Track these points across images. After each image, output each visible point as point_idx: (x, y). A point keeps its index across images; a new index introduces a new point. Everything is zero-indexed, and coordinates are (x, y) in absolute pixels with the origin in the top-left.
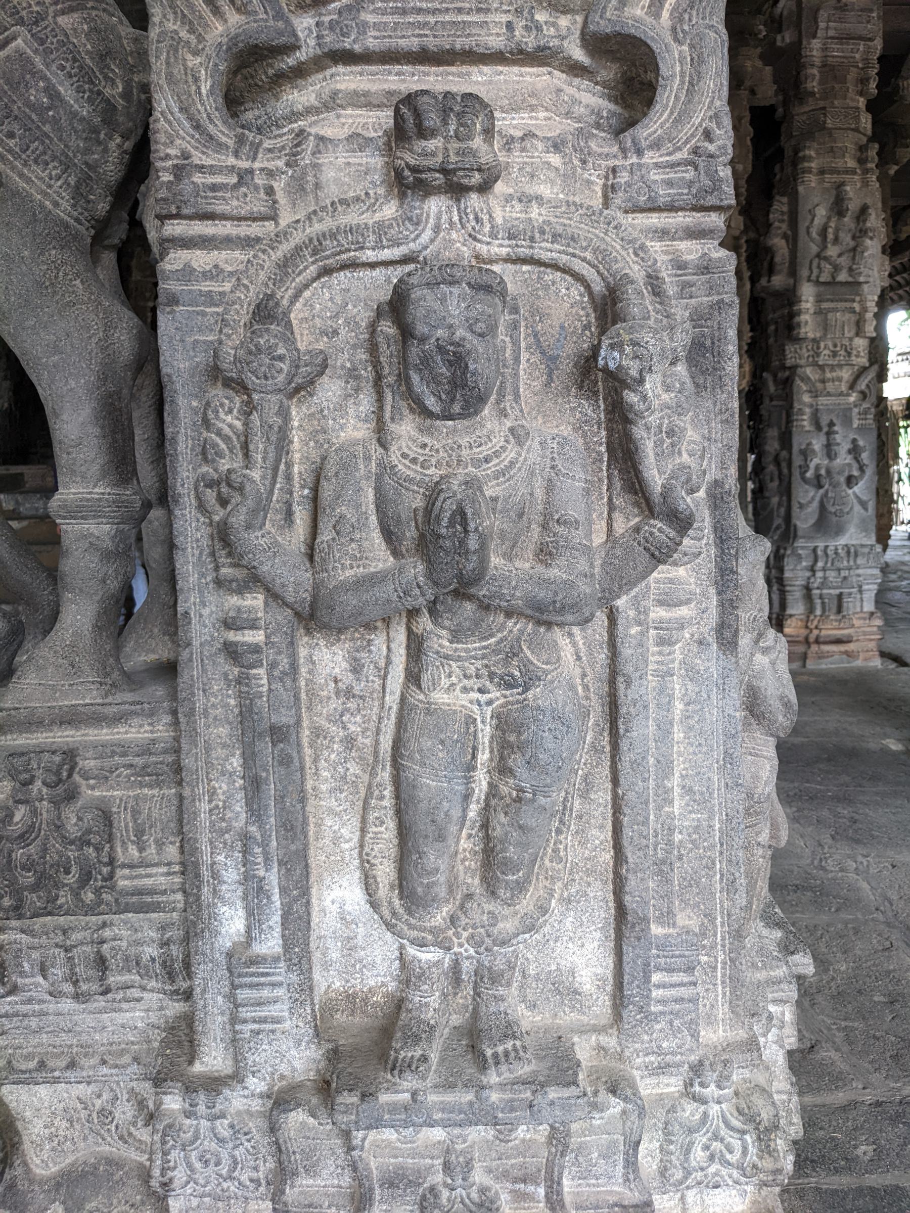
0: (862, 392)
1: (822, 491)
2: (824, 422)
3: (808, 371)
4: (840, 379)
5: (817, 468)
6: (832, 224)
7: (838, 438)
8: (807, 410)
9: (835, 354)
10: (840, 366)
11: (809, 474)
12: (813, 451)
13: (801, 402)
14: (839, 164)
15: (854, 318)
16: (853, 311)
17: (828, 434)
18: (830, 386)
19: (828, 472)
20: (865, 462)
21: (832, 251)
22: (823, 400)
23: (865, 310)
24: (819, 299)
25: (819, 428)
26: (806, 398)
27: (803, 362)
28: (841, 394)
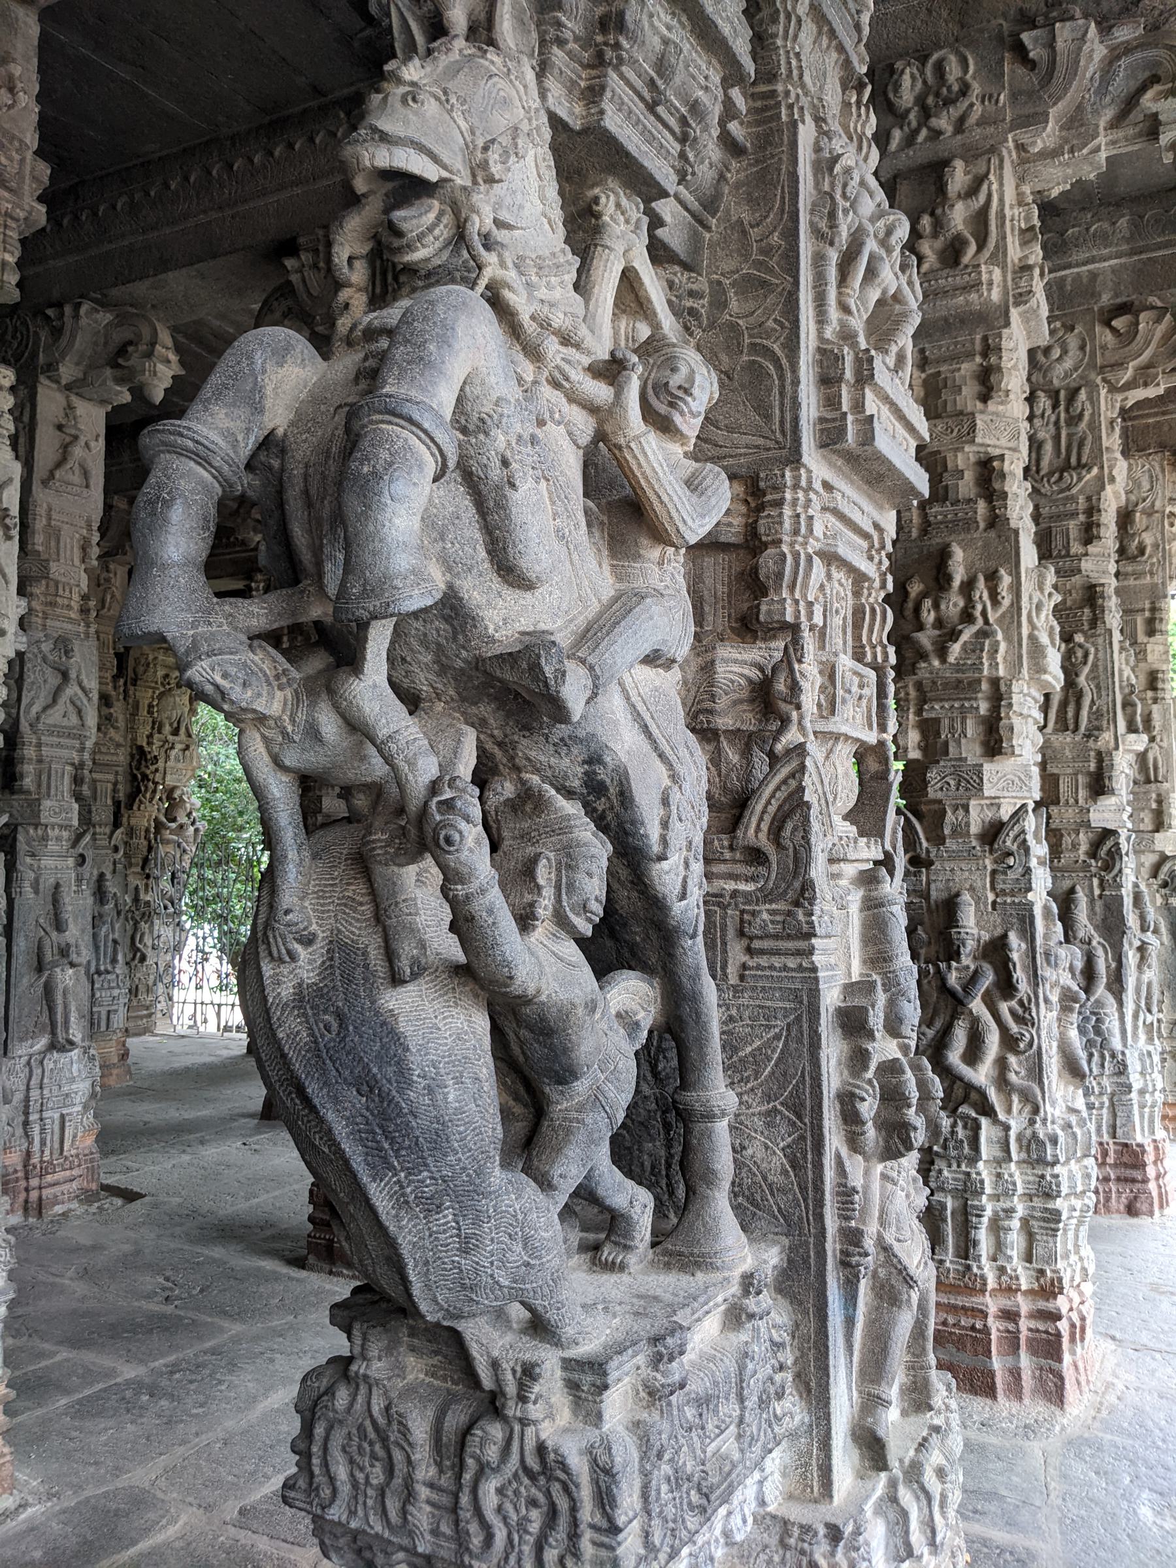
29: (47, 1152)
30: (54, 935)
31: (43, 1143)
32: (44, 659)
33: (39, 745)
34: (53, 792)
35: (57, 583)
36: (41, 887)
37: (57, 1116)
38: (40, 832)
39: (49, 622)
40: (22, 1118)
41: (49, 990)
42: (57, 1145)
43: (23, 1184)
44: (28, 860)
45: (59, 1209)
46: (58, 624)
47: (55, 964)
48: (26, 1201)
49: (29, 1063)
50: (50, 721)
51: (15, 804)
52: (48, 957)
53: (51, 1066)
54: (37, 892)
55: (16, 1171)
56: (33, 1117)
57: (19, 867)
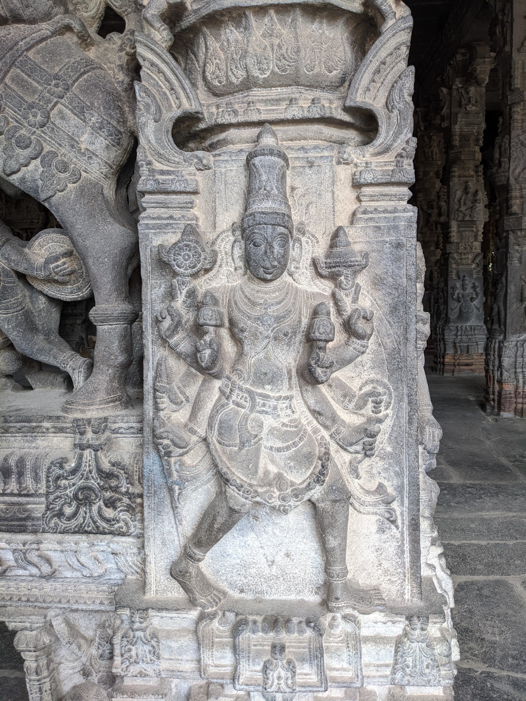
1: (460, 304)
2: (461, 275)
3: (455, 255)
4: (468, 258)
5: (458, 294)
6: (463, 198)
7: (467, 282)
8: (454, 271)
9: (465, 248)
10: (468, 253)
11: (455, 297)
12: (456, 287)
13: (452, 268)
14: (467, 173)
15: (474, 234)
16: (473, 231)
17: (463, 280)
18: (464, 262)
19: (463, 296)
21: (463, 208)
22: (461, 267)
23: (478, 231)
24: (459, 227)
25: (459, 278)
26: (454, 266)
27: (453, 251)
28: (468, 264)
40: (514, 370)
43: (514, 400)
48: (516, 408)
49: (516, 345)
51: (511, 220)
55: (510, 394)
56: (519, 370)
57: (510, 251)
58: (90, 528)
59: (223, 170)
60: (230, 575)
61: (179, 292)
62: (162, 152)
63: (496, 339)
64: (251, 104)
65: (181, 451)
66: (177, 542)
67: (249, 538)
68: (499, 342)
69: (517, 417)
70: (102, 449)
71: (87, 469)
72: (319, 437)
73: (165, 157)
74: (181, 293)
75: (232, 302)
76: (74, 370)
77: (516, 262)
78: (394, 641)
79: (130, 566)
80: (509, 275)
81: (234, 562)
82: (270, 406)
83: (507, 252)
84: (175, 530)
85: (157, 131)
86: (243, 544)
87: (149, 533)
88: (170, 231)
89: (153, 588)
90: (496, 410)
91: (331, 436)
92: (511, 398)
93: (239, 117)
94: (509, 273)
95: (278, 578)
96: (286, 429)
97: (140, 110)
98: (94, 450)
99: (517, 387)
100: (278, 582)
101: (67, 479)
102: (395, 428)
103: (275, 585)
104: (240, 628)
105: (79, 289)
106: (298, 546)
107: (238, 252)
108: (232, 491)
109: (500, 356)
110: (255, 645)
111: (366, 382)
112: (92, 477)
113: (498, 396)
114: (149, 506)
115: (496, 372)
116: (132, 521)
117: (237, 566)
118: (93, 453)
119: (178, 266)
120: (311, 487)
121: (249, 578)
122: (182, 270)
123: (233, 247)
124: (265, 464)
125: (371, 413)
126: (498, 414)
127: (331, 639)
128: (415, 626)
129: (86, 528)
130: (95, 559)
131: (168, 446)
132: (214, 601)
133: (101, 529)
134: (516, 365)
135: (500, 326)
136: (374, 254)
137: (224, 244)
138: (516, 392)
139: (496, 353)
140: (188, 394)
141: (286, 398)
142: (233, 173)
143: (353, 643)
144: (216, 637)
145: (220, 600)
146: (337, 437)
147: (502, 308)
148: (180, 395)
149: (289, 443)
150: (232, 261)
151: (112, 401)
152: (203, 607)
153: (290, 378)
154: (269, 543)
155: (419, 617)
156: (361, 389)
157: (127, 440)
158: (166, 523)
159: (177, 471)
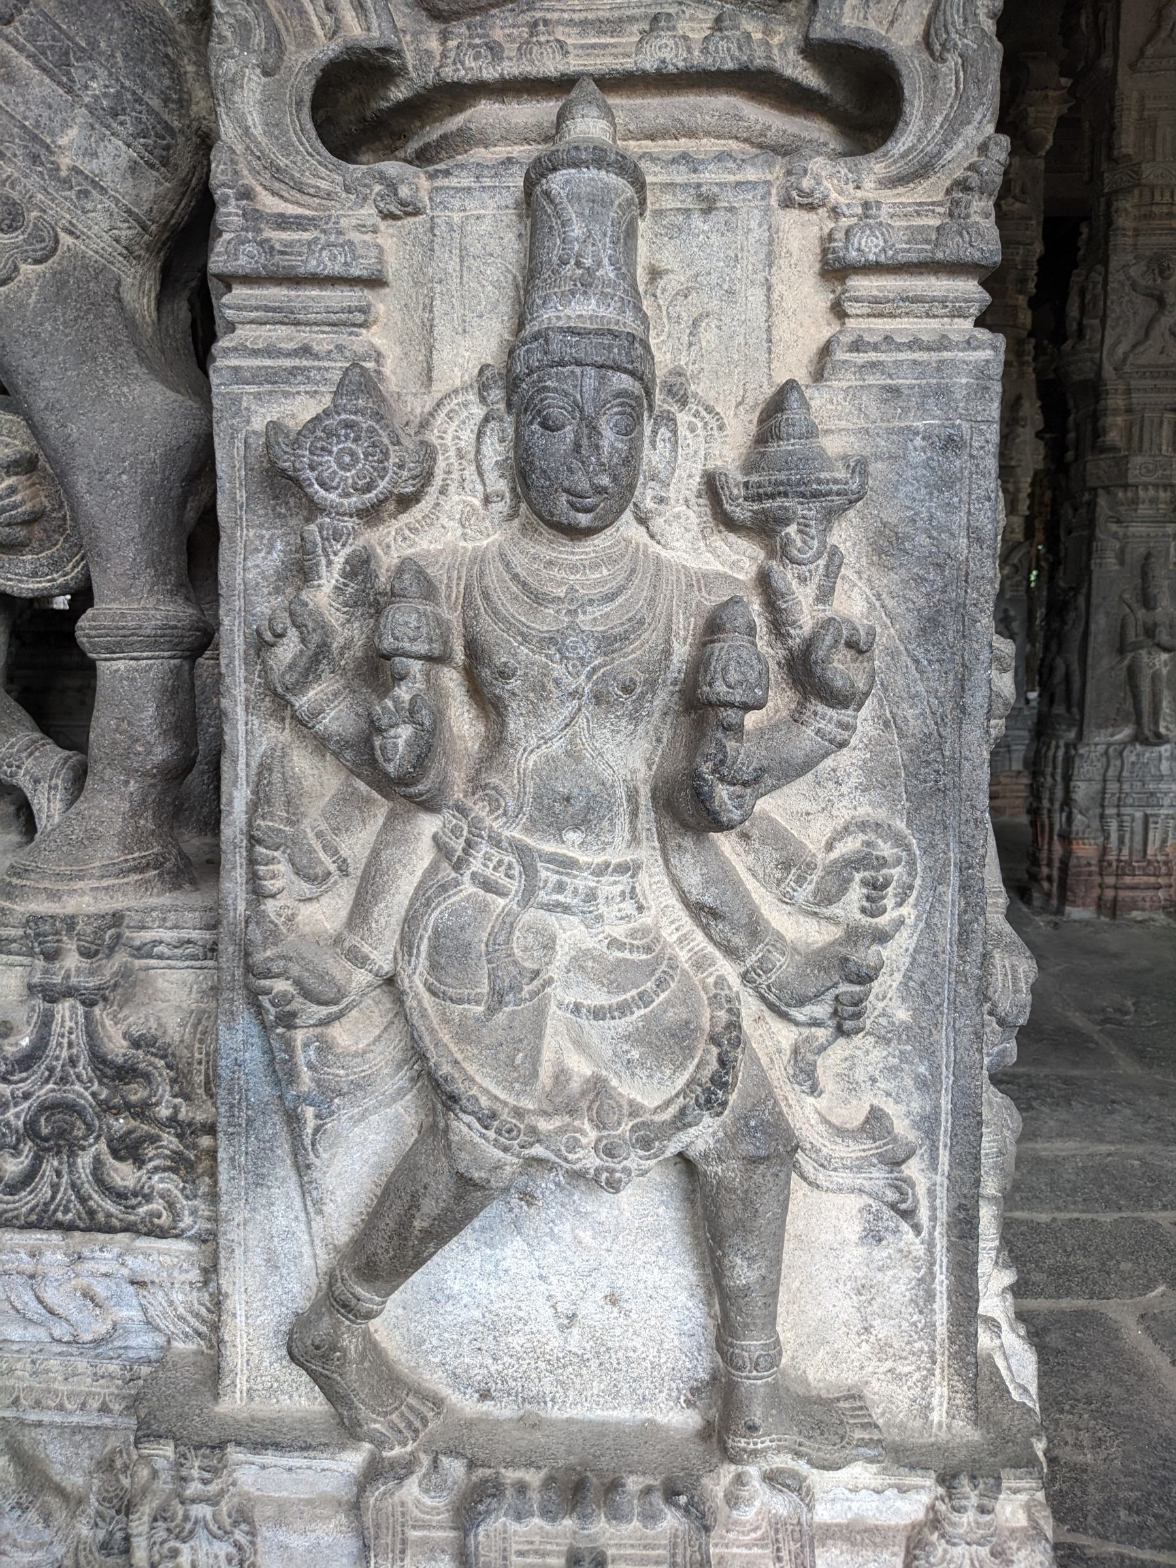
0: (1014, 566)
20: (1016, 630)
29: (1125, 852)
30: (1141, 613)
31: (1121, 841)
32: (1134, 286)
33: (1128, 391)
34: (1146, 445)
35: (1152, 188)
36: (1128, 557)
37: (1139, 815)
38: (1130, 494)
39: (1142, 240)
40: (1098, 811)
41: (1132, 674)
42: (1138, 846)
43: (1097, 879)
44: (1114, 527)
45: (1137, 915)
46: (1154, 240)
47: (1137, 646)
48: (1100, 898)
49: (1106, 753)
50: (1143, 361)
52: (1131, 637)
53: (1133, 758)
54: (1122, 562)
55: (1089, 865)
58: (70, 1216)
59: (457, 217)
60: (451, 1352)
61: (324, 561)
62: (282, 162)
63: (1058, 738)
64: (541, 28)
65: (324, 1011)
66: (308, 1261)
67: (508, 1252)
68: (1067, 746)
69: (1103, 918)
70: (105, 999)
71: (65, 1054)
72: (711, 980)
73: (292, 178)
74: (330, 563)
75: (477, 594)
76: (37, 781)
77: (1111, 561)
78: (901, 1539)
79: (181, 1318)
80: (1094, 592)
81: (465, 1315)
82: (575, 892)
83: (1091, 538)
84: (303, 1227)
85: (269, 99)
86: (490, 1267)
87: (231, 1234)
88: (302, 388)
89: (242, 1383)
90: (1054, 902)
91: (744, 976)
92: (1090, 874)
93: (506, 63)
94: (1094, 586)
95: (584, 1361)
96: (620, 955)
97: (222, 39)
98: (83, 1003)
99: (1104, 850)
100: (584, 1371)
101: (9, 1082)
102: (921, 958)
103: (578, 1381)
104: (481, 1508)
105: (56, 564)
106: (644, 1275)
107: (494, 451)
108: (465, 1129)
109: (1067, 778)
110: (521, 1554)
111: (846, 829)
112: (78, 1077)
113: (1060, 869)
114: (232, 1159)
115: (1057, 816)
116: (187, 1198)
117: (472, 1328)
118: (81, 1010)
119: (322, 485)
120: (689, 1119)
121: (506, 1359)
122: (333, 496)
123: (480, 435)
124: (559, 1051)
125: (858, 915)
126: (1060, 911)
127: (731, 1535)
128: (964, 1502)
129: (59, 1215)
130: (85, 1295)
131: (286, 998)
132: (410, 1425)
133: (101, 1217)
134: (1103, 799)
135: (1069, 709)
136: (880, 465)
137: (454, 426)
138: (1101, 861)
139: (1059, 771)
140: (344, 852)
141: (622, 869)
142: (486, 226)
143: (794, 1547)
144: (414, 1527)
145: (424, 1421)
146: (763, 980)
147: (1075, 667)
148: (322, 855)
149: (628, 996)
150: (475, 477)
151: (135, 869)
152: (380, 1442)
153: (634, 814)
154: (564, 1268)
155: (973, 1478)
156: (830, 847)
157: (175, 975)
158: (279, 1208)
159: (311, 1066)
